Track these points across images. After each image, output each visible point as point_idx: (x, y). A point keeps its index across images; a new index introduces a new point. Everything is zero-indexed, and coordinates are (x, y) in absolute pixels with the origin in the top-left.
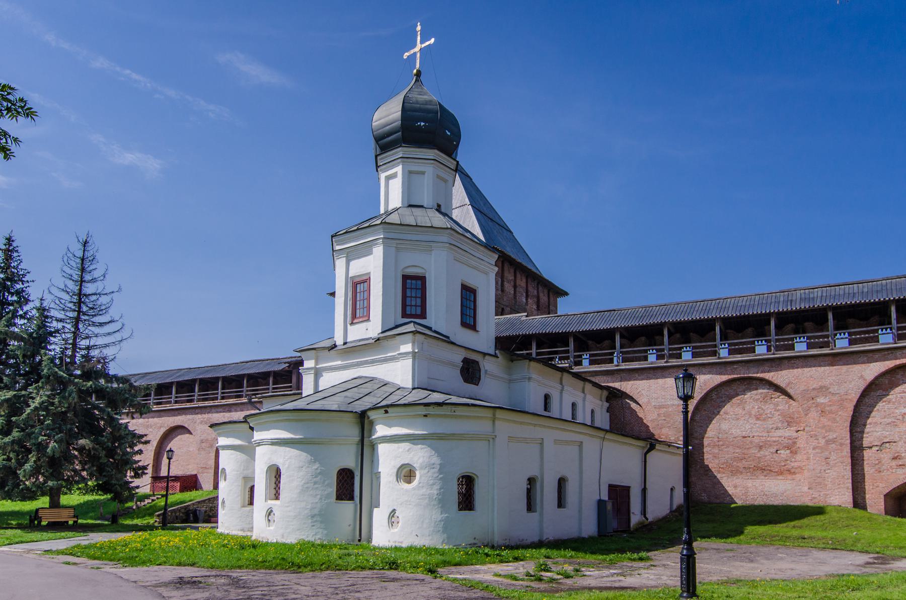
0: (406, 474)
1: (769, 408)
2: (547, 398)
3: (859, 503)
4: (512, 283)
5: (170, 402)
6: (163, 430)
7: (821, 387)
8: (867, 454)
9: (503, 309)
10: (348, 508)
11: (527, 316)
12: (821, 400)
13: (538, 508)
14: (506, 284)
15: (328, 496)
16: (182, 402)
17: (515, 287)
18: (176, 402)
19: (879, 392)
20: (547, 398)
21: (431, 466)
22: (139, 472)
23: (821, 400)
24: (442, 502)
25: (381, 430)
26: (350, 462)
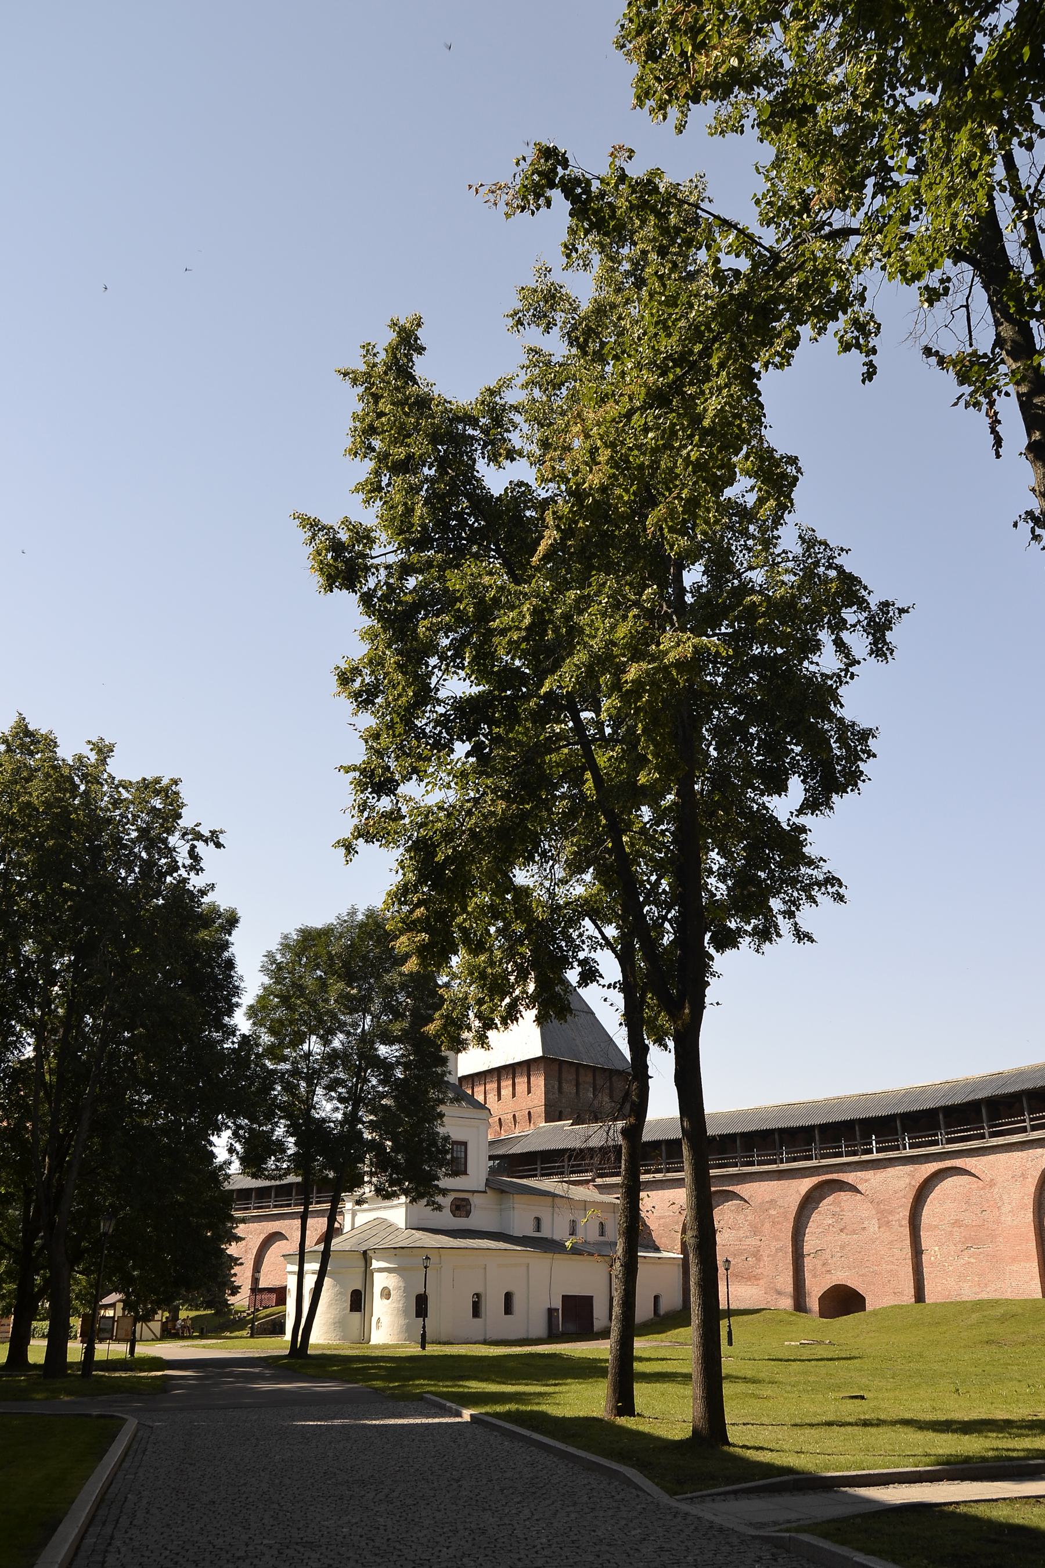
0: (386, 1294)
1: (740, 1218)
2: (538, 1220)
3: (800, 1305)
4: (574, 1083)
5: (268, 1207)
6: (263, 1237)
7: (772, 1200)
8: (806, 1260)
9: (561, 1112)
10: (357, 1315)
11: (572, 1125)
12: (773, 1212)
13: (483, 1315)
14: (565, 1086)
15: (344, 1309)
16: (281, 1206)
17: (577, 1085)
18: (275, 1206)
19: (814, 1205)
20: (538, 1220)
21: (399, 1288)
22: (235, 1290)
23: (773, 1212)
24: (405, 1312)
25: (376, 1264)
26: (359, 1286)
